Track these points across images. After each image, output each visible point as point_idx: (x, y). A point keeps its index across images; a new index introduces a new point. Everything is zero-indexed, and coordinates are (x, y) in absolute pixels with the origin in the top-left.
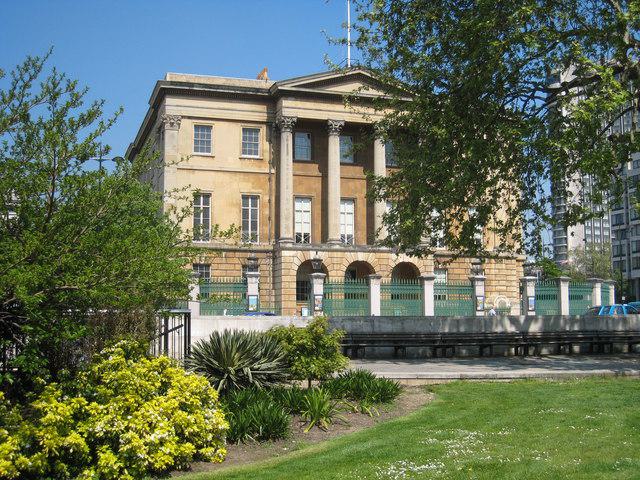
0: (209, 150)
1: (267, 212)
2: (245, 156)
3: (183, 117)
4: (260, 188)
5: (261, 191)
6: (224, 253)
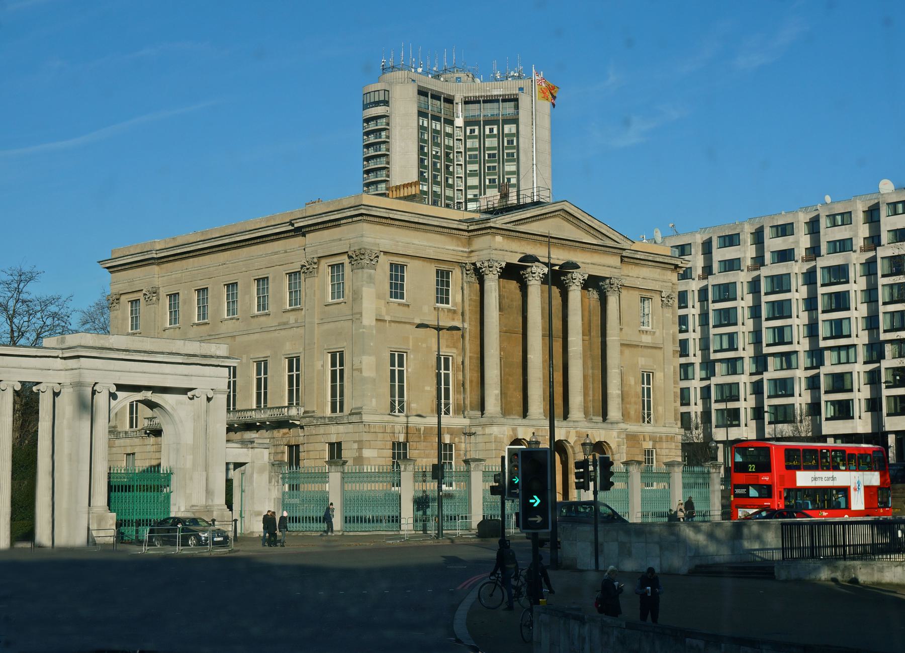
1: (461, 377)
2: (439, 305)
4: (455, 347)
5: (455, 351)
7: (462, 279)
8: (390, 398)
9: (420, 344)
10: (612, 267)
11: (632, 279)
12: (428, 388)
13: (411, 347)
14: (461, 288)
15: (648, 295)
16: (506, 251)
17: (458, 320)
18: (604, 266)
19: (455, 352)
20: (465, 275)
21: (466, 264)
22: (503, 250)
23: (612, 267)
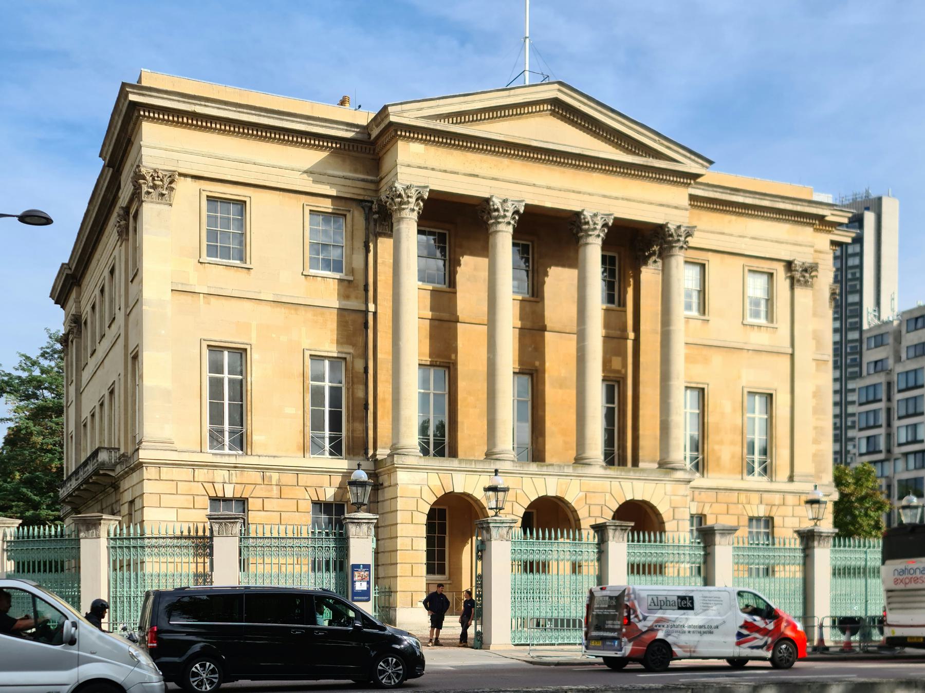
0: (242, 258)
3: (181, 175)
6: (275, 476)
7: (367, 229)
8: (208, 425)
9: (274, 336)
10: (668, 206)
11: (733, 239)
12: (290, 411)
13: (253, 342)
14: (363, 244)
15: (766, 266)
16: (433, 169)
17: (357, 298)
18: (651, 203)
19: (351, 351)
20: (372, 224)
21: (372, 202)
22: (426, 168)
23: (668, 206)
